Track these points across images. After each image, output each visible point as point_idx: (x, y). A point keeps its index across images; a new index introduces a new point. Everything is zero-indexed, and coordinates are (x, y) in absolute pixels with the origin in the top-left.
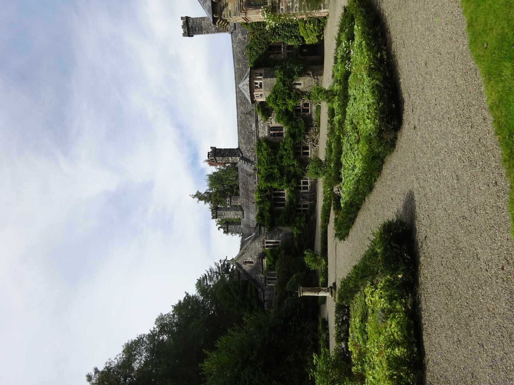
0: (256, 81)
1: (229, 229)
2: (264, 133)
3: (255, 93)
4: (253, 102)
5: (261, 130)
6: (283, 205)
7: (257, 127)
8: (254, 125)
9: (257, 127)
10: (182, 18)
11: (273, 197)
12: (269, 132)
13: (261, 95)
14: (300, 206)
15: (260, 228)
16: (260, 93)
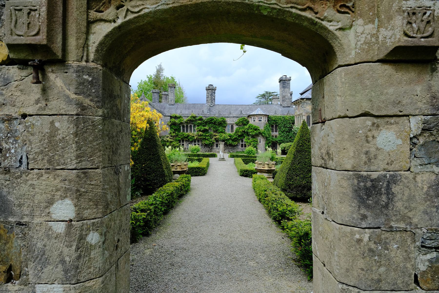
0: (262, 118)
1: (155, 94)
2: (229, 121)
3: (256, 117)
4: (249, 116)
5: (232, 119)
6: (184, 131)
7: (234, 117)
8: (235, 115)
9: (234, 117)
10: (290, 77)
11: (189, 125)
12: (230, 124)
13: (254, 121)
14: (183, 142)
15: (169, 116)
16: (256, 120)
